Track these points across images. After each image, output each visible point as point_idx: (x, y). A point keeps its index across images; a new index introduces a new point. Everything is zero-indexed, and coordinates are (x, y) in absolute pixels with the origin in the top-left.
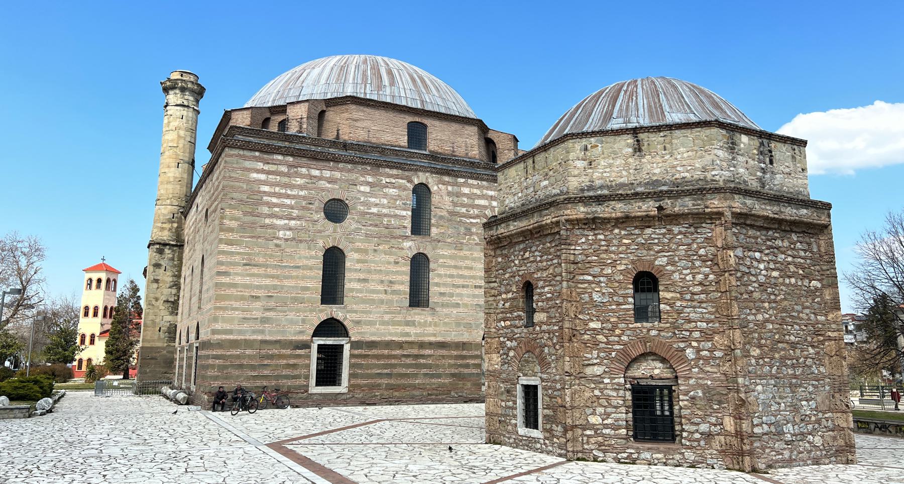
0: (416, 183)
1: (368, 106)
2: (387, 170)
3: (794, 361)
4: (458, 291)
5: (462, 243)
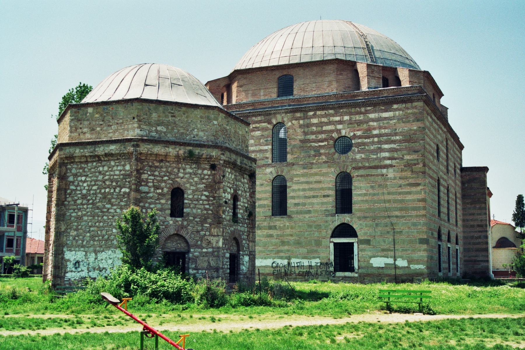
0: (275, 123)
1: (249, 73)
2: (254, 118)
3: (101, 238)
4: (309, 201)
5: (312, 164)
